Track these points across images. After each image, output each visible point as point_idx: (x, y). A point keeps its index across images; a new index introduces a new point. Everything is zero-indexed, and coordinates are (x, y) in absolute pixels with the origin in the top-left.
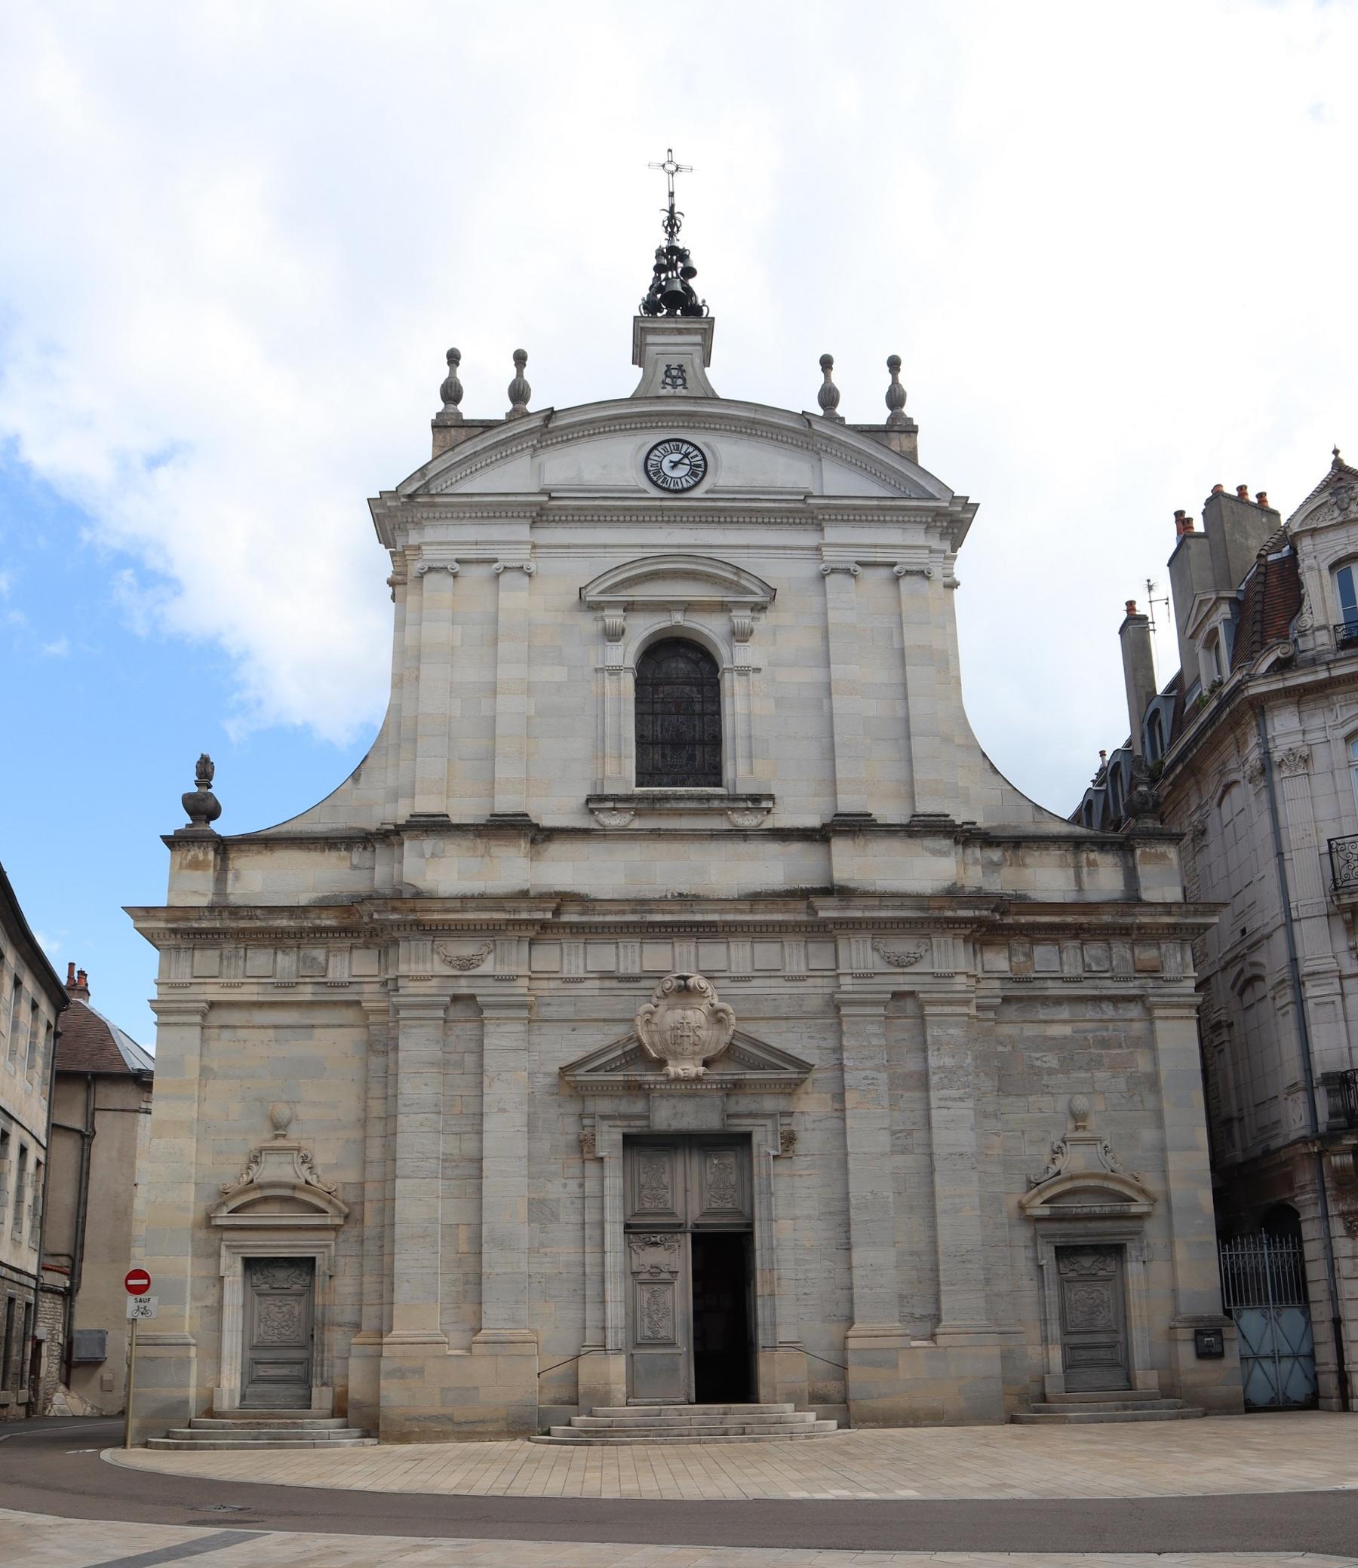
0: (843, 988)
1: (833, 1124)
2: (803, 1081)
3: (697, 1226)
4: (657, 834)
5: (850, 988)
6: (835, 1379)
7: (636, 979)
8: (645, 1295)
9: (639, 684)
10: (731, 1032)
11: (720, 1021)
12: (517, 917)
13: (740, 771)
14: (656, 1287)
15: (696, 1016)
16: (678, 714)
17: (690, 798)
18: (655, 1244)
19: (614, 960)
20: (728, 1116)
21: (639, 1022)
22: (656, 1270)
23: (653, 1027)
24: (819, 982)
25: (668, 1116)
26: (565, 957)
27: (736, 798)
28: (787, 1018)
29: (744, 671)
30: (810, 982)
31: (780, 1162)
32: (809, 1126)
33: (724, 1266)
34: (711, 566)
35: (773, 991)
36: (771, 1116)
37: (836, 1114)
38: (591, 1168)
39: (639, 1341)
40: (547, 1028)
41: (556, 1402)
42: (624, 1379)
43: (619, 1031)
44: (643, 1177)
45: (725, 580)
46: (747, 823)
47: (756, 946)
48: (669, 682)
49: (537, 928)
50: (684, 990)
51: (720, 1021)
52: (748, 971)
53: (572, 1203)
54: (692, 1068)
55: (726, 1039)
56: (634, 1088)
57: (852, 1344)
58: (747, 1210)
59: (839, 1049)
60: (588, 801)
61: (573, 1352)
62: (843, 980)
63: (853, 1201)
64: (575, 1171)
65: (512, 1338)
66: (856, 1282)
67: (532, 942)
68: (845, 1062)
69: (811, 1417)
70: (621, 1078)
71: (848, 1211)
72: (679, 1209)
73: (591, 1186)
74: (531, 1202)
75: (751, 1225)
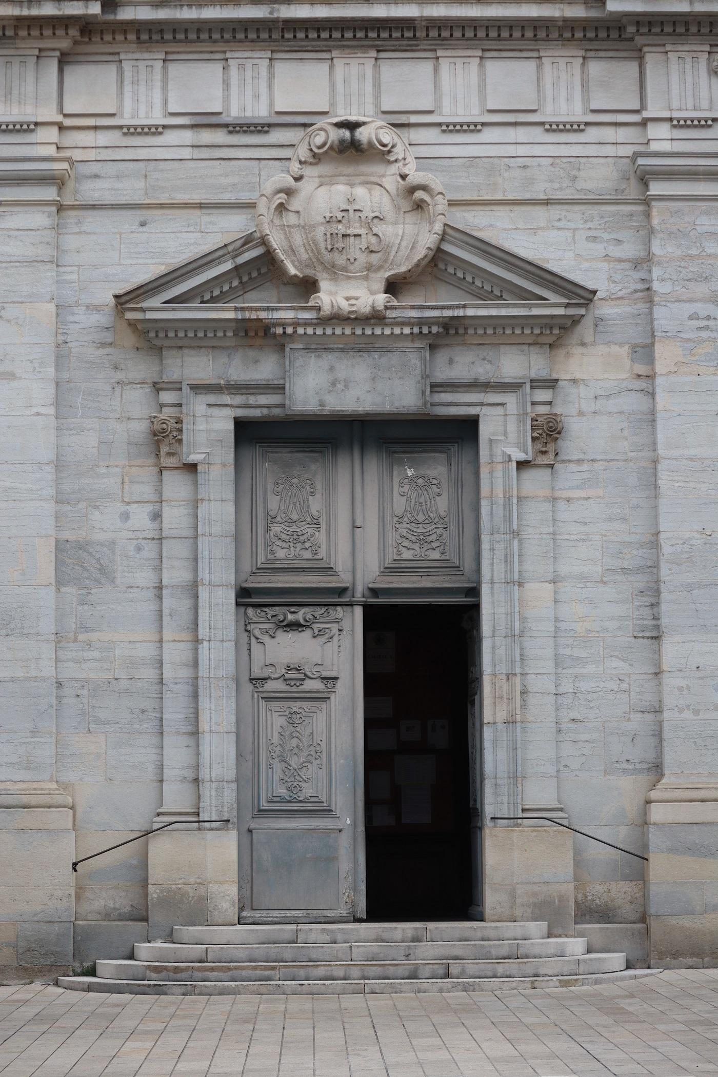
0: (654, 147)
1: (634, 402)
2: (576, 321)
3: (374, 592)
5: (666, 147)
6: (625, 878)
7: (262, 128)
8: (275, 721)
10: (438, 228)
11: (419, 206)
12: (35, 12)
14: (295, 706)
15: (369, 194)
18: (295, 626)
19: (219, 92)
20: (436, 387)
21: (262, 207)
22: (296, 673)
23: (292, 219)
24: (609, 134)
25: (321, 385)
26: (128, 88)
28: (547, 202)
30: (592, 134)
31: (530, 475)
32: (584, 407)
33: (424, 661)
35: (522, 150)
36: (513, 387)
37: (642, 384)
38: (176, 486)
39: (264, 804)
40: (92, 220)
41: (107, 916)
42: (233, 874)
43: (232, 226)
44: (274, 503)
47: (489, 64)
49: (74, 32)
50: (351, 149)
51: (419, 206)
52: (474, 115)
53: (139, 549)
54: (366, 296)
55: (427, 240)
56: (256, 334)
57: (657, 813)
58: (468, 565)
59: (644, 261)
61: (139, 823)
62: (654, 131)
63: (666, 549)
64: (146, 490)
65: (25, 800)
66: (669, 700)
67: (64, 60)
68: (656, 286)
69: (575, 946)
70: (231, 315)
71: (656, 566)
72: (341, 561)
73: (175, 517)
74: (60, 547)
75: (474, 592)
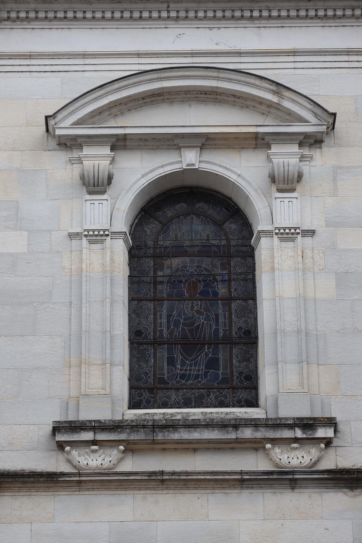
4: (159, 481)
9: (135, 255)
13: (283, 385)
16: (192, 299)
17: (210, 424)
27: (277, 424)
29: (288, 235)
34: (239, 82)
45: (261, 101)
46: (295, 462)
48: (179, 251)
60: (57, 429)
